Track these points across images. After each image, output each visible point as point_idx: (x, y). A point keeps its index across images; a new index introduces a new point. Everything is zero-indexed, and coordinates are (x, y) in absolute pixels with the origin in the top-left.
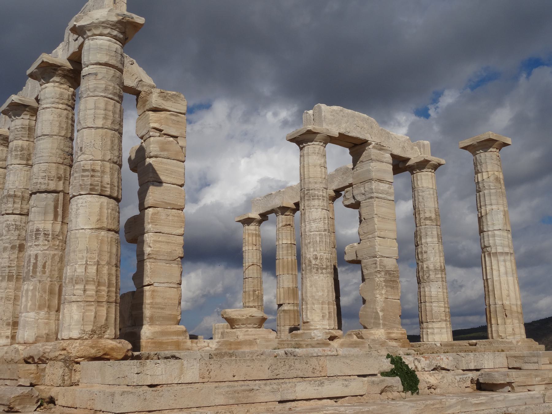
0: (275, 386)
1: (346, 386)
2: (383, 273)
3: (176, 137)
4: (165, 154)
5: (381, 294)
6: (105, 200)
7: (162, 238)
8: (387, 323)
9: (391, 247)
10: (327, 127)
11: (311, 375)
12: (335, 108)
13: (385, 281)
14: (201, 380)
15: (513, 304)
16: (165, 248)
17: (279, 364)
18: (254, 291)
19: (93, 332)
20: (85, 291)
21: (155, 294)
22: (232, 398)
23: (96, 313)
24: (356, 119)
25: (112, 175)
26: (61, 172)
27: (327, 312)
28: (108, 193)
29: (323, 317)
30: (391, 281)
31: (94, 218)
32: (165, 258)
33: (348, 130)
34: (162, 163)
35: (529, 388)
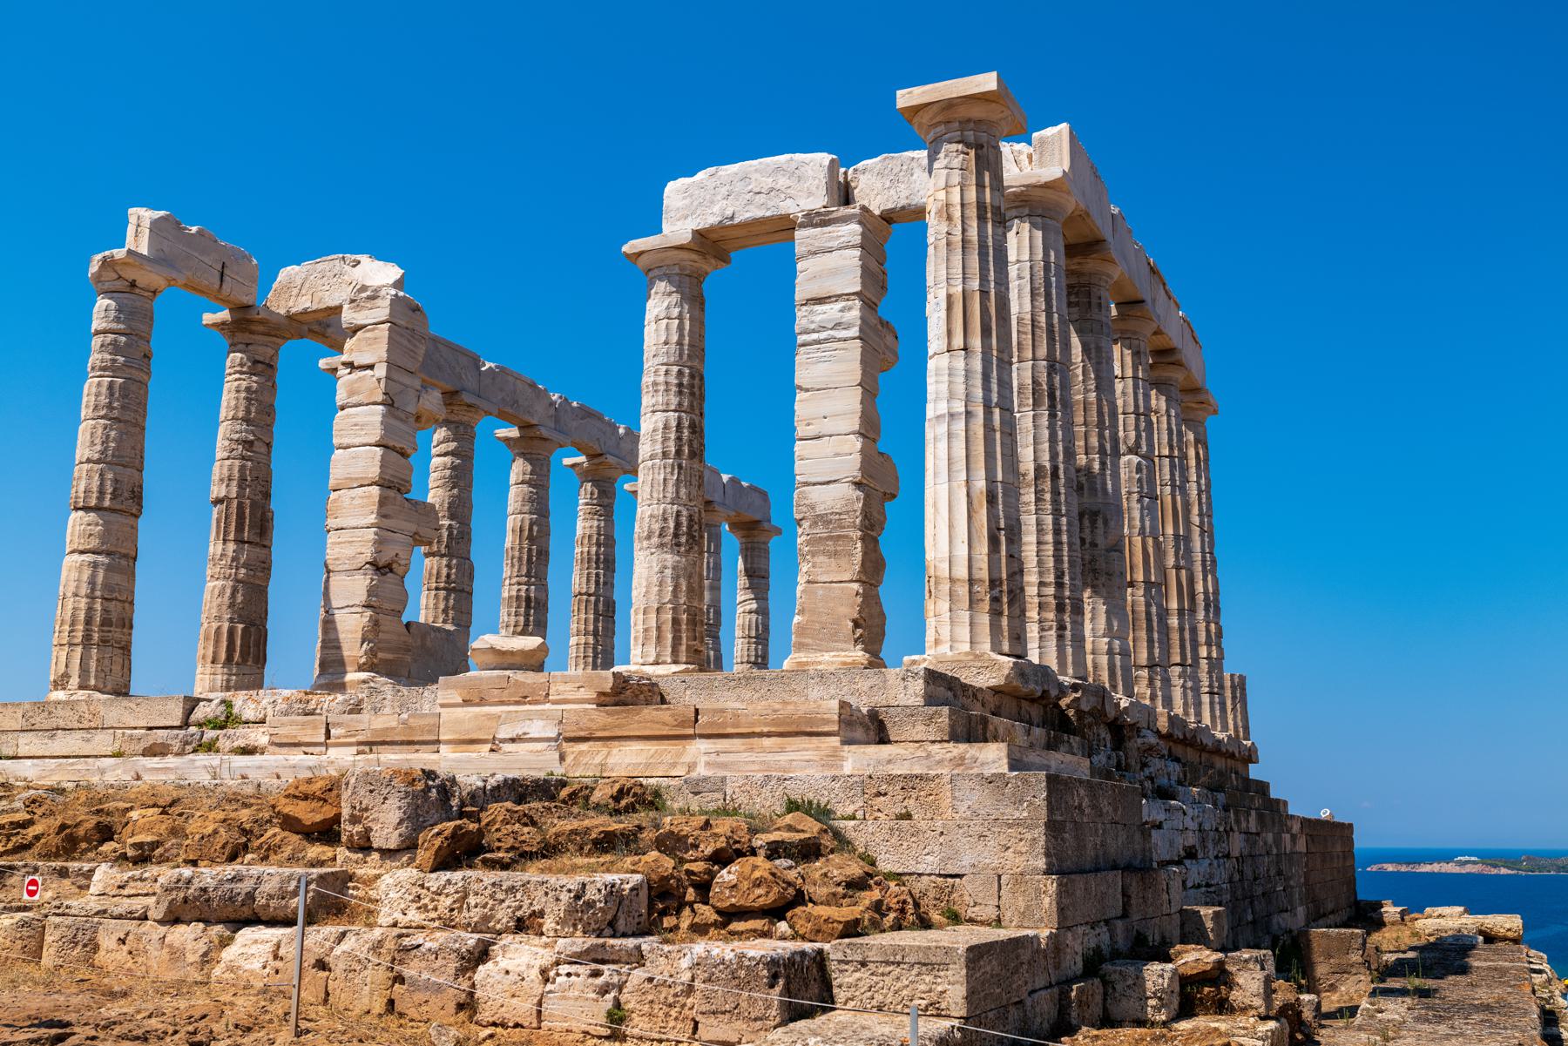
3: (371, 367)
4: (354, 400)
6: (81, 513)
7: (345, 536)
9: (837, 455)
11: (76, 725)
12: (701, 175)
16: (349, 551)
25: (89, 477)
26: (225, 471)
30: (830, 538)
33: (729, 213)
34: (348, 416)
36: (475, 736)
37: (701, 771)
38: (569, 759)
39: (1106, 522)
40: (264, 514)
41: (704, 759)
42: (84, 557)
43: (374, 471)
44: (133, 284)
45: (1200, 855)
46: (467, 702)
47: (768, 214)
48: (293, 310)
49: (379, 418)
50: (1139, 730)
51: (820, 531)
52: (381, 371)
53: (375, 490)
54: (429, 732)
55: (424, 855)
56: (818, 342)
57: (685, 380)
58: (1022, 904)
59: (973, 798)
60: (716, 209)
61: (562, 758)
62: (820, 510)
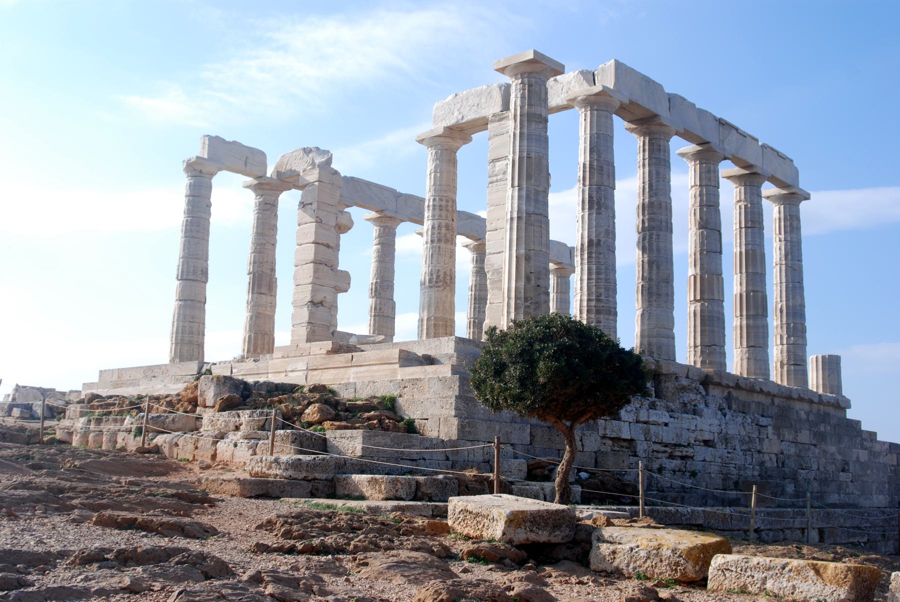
3: (311, 204)
37: (351, 381)
39: (658, 268)
40: (271, 279)
41: (352, 376)
43: (311, 257)
44: (201, 172)
45: (719, 445)
46: (283, 357)
49: (313, 230)
50: (676, 378)
52: (315, 206)
53: (312, 265)
55: (217, 406)
57: (444, 203)
58: (446, 430)
59: (437, 386)
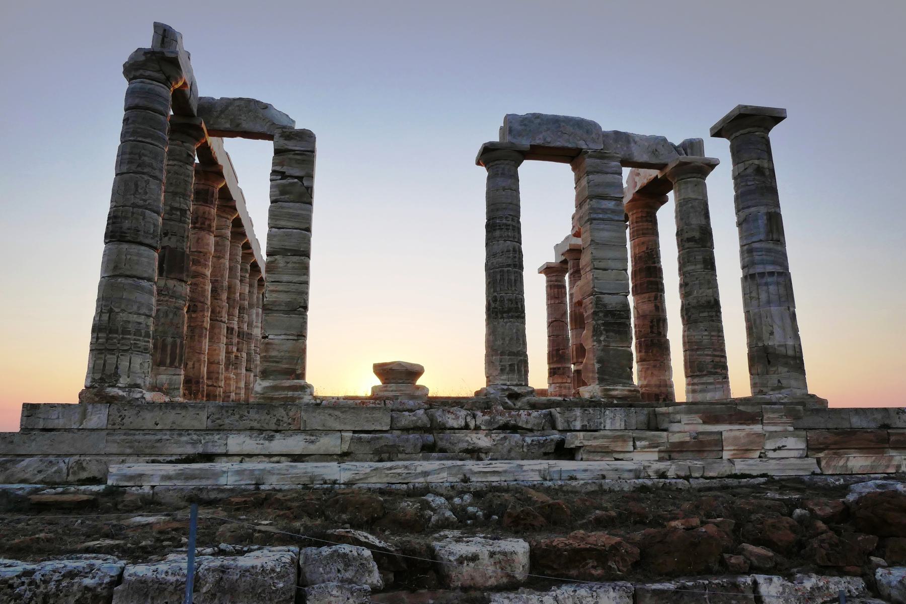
0: (195, 437)
1: (312, 442)
2: (601, 315)
3: (300, 178)
5: (599, 342)
8: (606, 377)
10: (514, 141)
13: (603, 324)
14: (110, 426)
15: (779, 346)
16: (284, 298)
17: (224, 412)
18: (558, 350)
19: (102, 380)
20: (98, 338)
21: (269, 346)
22: (131, 447)
23: (105, 361)
24: (563, 124)
27: (507, 364)
28: (129, 238)
29: (502, 370)
30: (616, 323)
31: (112, 266)
32: (282, 308)
33: (549, 140)
34: (282, 207)
35: (617, 456)
36: (750, 448)
38: (823, 463)
42: (130, 281)
46: (704, 423)
47: (570, 146)
48: (216, 127)
51: (610, 319)
54: (716, 445)
56: (603, 220)
60: (541, 136)
61: (819, 462)
62: (609, 308)
